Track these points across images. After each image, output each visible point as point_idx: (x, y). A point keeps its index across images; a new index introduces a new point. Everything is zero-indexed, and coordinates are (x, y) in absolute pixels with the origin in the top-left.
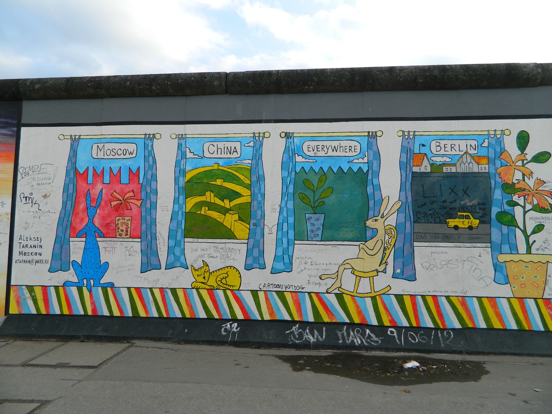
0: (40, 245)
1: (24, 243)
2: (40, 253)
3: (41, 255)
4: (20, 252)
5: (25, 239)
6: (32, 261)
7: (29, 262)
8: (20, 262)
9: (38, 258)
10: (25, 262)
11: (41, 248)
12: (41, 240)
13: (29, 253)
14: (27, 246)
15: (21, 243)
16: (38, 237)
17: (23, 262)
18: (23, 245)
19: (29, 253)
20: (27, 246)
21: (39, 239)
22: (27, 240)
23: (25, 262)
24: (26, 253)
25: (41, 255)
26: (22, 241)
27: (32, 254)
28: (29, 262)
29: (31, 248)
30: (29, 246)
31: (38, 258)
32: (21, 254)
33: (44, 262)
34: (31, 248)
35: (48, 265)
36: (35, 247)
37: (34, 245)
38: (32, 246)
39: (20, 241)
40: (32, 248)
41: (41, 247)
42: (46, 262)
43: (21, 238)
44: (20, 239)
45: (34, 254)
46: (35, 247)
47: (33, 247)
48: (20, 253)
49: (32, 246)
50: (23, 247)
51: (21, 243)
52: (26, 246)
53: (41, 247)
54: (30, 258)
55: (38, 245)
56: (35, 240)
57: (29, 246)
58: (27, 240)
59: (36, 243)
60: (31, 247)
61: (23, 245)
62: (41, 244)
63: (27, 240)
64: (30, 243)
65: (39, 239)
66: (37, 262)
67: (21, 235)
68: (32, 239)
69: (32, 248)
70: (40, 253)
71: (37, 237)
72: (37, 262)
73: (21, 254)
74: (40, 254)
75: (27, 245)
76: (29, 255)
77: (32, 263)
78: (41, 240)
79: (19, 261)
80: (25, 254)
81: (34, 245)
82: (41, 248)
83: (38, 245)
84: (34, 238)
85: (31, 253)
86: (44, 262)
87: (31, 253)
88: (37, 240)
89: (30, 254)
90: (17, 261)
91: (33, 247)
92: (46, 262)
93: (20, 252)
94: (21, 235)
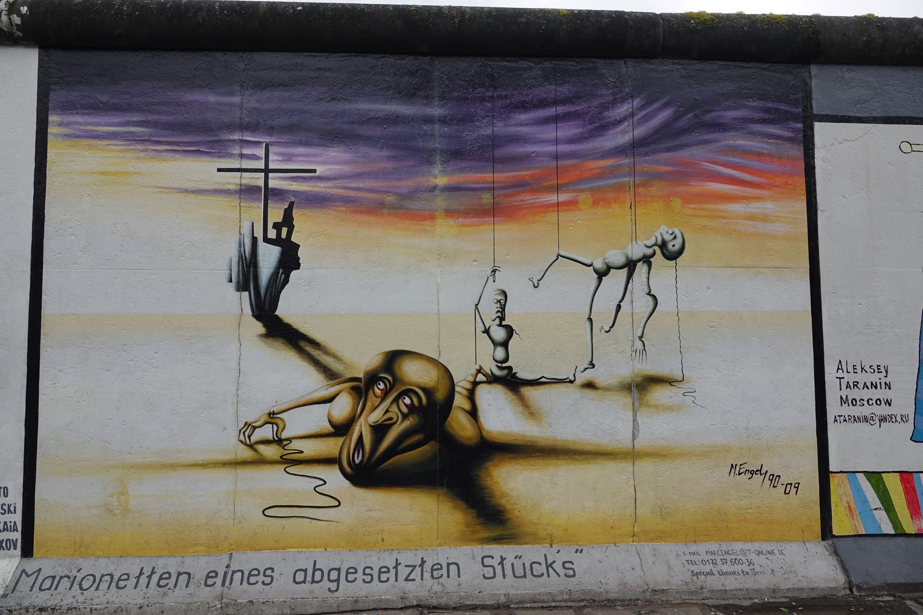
0: (886, 383)
1: (850, 378)
2: (887, 400)
3: (890, 405)
4: (841, 398)
5: (851, 369)
6: (873, 417)
7: (866, 419)
8: (845, 421)
9: (883, 410)
10: (856, 419)
11: (890, 388)
12: (887, 372)
13: (872, 400)
14: (856, 384)
15: (843, 378)
16: (880, 366)
17: (852, 420)
18: (848, 382)
19: (863, 400)
20: (856, 385)
21: (883, 370)
22: (855, 371)
23: (856, 419)
24: (856, 401)
25: (890, 405)
26: (845, 375)
27: (870, 402)
28: (866, 419)
29: (865, 388)
30: (861, 386)
31: (883, 410)
32: (845, 403)
33: (899, 419)
34: (865, 388)
35: (909, 427)
36: (876, 388)
37: (872, 383)
38: (869, 385)
39: (840, 374)
40: (868, 389)
41: (888, 386)
42: (904, 419)
43: (840, 367)
44: (838, 369)
45: (874, 402)
46: (876, 388)
47: (870, 387)
48: (843, 401)
49: (869, 385)
50: (847, 387)
51: (843, 378)
52: (854, 385)
53: (888, 386)
54: (866, 411)
55: (880, 383)
56: (872, 371)
57: (861, 386)
58: (854, 373)
59: (875, 378)
60: (865, 385)
61: (848, 382)
62: (887, 381)
63: (855, 371)
64: (862, 378)
65: (883, 370)
66: (883, 419)
67: (840, 361)
68: (867, 368)
69: (868, 389)
70: (887, 400)
71: (878, 366)
72: (883, 419)
73: (845, 403)
74: (888, 403)
75: (858, 383)
76: (863, 405)
77: (871, 422)
78: (887, 372)
79: (842, 419)
80: (854, 404)
81: (872, 383)
82: (890, 388)
83: (880, 383)
84: (870, 367)
85: (868, 401)
86: (899, 419)
87: (868, 401)
88: (879, 372)
89: (865, 403)
90: (838, 418)
91: (870, 387)
92: (904, 419)
93: (841, 398)
94: (840, 361)
